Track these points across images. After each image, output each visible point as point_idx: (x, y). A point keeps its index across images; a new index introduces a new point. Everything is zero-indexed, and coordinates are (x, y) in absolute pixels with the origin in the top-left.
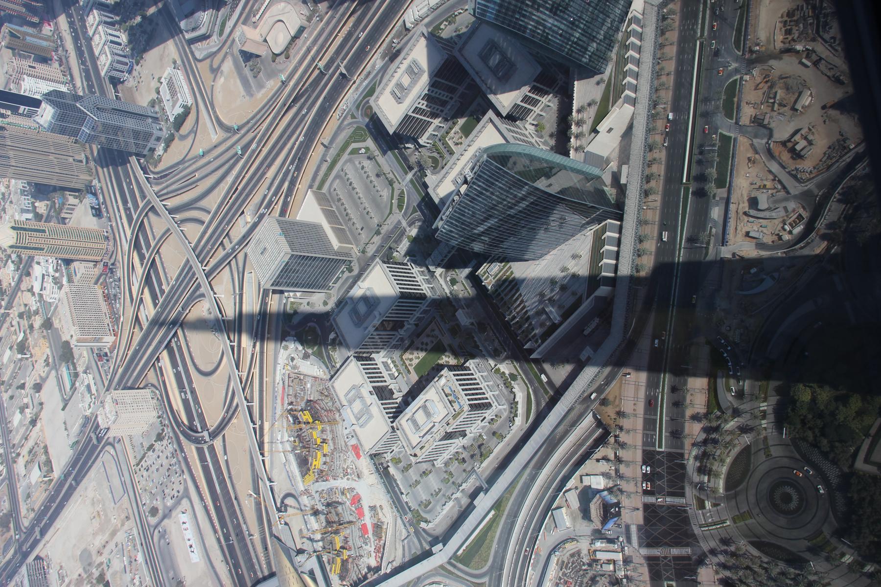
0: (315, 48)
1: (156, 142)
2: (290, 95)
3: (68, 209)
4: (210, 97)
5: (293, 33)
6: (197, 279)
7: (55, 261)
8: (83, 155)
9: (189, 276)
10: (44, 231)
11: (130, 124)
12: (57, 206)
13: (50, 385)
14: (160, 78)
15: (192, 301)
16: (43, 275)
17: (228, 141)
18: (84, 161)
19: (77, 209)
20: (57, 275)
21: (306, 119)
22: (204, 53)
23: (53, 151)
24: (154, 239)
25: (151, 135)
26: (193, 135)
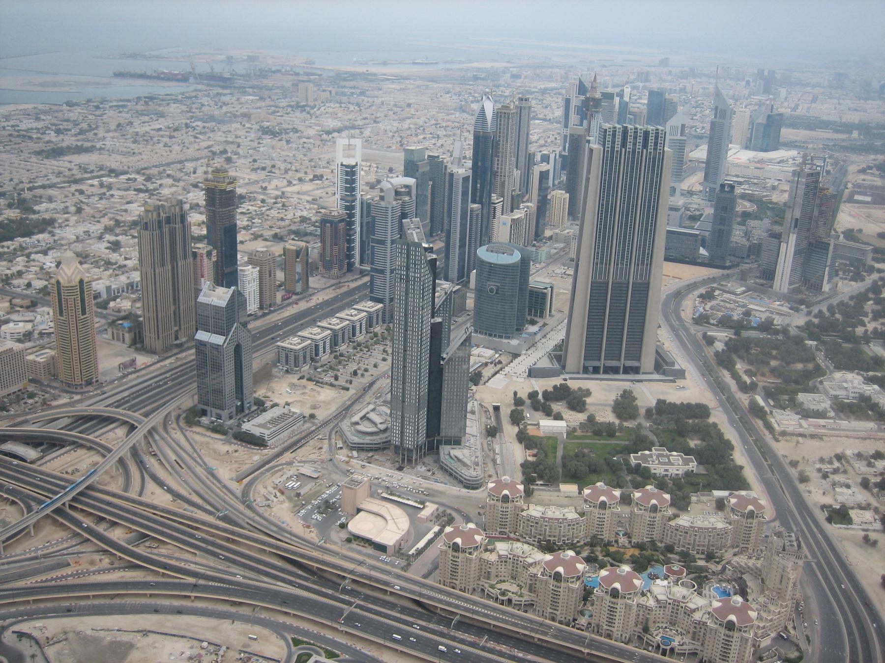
1: (214, 415)
2: (302, 556)
3: (118, 335)
5: (378, 539)
6: (51, 498)
7: (52, 330)
8: (184, 340)
9: (53, 488)
10: (84, 313)
11: (230, 382)
12: (120, 322)
15: (20, 499)
18: (178, 342)
19: (120, 344)
20: (36, 336)
21: (279, 583)
24: (96, 437)
25: (222, 408)
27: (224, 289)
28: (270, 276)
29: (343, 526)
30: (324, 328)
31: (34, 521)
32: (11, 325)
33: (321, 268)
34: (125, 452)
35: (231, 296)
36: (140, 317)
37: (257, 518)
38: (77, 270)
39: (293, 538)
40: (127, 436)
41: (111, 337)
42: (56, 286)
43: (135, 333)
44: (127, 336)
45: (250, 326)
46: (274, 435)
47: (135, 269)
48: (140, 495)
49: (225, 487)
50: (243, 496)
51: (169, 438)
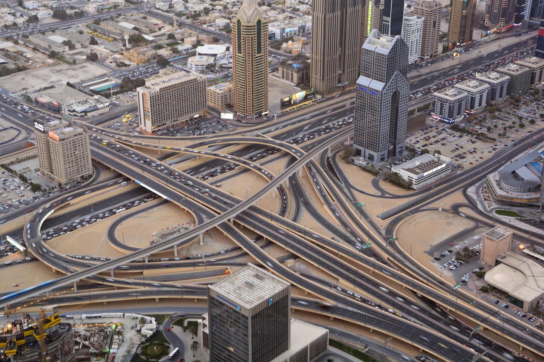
0: (497, 321)
3: (287, 73)
4: (425, 208)
6: (219, 214)
8: (346, 83)
10: (259, 51)
11: (385, 128)
13: (95, 70)
14: (439, 153)
15: (194, 211)
16: (215, 55)
17: (376, 233)
18: (340, 85)
19: (288, 82)
20: (217, 68)
21: (412, 319)
22: (474, 197)
23: (347, 53)
26: (380, 194)
27: (389, 38)
28: (434, 26)
29: (481, 276)
30: (482, 82)
31: (204, 231)
32: (197, 57)
33: (487, 21)
34: (285, 182)
35: (394, 45)
36: (309, 59)
37: (397, 255)
38: (256, 11)
39: (429, 278)
40: (288, 167)
41: (281, 76)
42: (236, 25)
43: (303, 74)
44: (295, 75)
45: (408, 76)
46: (420, 180)
47: (308, 14)
48: (295, 220)
49: (371, 223)
50: (387, 234)
51: (324, 173)
